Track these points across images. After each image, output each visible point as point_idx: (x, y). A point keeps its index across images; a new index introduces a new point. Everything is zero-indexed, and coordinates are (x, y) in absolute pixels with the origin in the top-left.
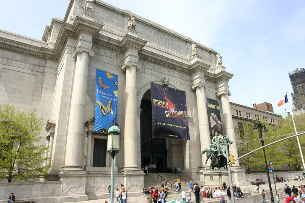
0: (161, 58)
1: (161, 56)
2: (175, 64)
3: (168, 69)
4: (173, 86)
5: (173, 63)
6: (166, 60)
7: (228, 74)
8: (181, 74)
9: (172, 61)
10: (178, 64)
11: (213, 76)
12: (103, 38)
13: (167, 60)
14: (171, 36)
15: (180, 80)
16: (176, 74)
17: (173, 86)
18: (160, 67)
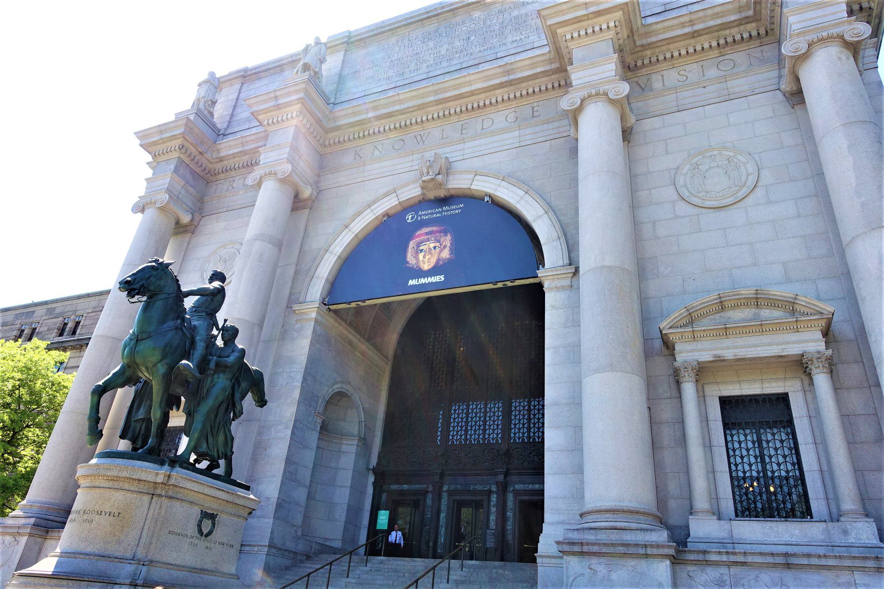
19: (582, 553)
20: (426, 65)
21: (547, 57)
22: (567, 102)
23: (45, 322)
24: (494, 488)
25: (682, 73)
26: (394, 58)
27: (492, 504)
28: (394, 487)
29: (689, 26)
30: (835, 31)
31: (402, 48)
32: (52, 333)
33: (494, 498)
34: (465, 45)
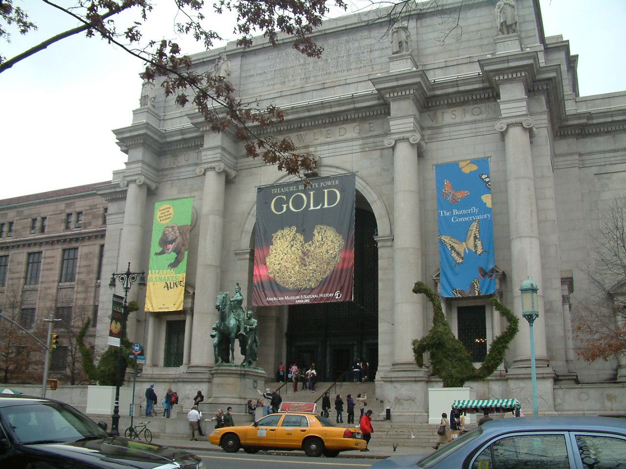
0: (293, 113)
1: (291, 111)
2: (334, 109)
3: (327, 129)
4: (337, 168)
5: (327, 111)
6: (307, 114)
7: (508, 61)
8: (366, 126)
9: (324, 108)
10: (344, 105)
11: (477, 82)
12: (172, 136)
13: (309, 111)
14: (343, 34)
15: (360, 142)
16: (351, 131)
17: (337, 168)
18: (302, 133)
19: (391, 381)
20: (299, 78)
21: (376, 96)
22: (388, 142)
23: (18, 222)
24: (355, 343)
25: (454, 112)
26: (277, 69)
27: (355, 350)
28: (299, 344)
29: (456, 87)
30: (518, 120)
31: (282, 60)
32: (27, 231)
33: (355, 348)
34: (325, 65)
